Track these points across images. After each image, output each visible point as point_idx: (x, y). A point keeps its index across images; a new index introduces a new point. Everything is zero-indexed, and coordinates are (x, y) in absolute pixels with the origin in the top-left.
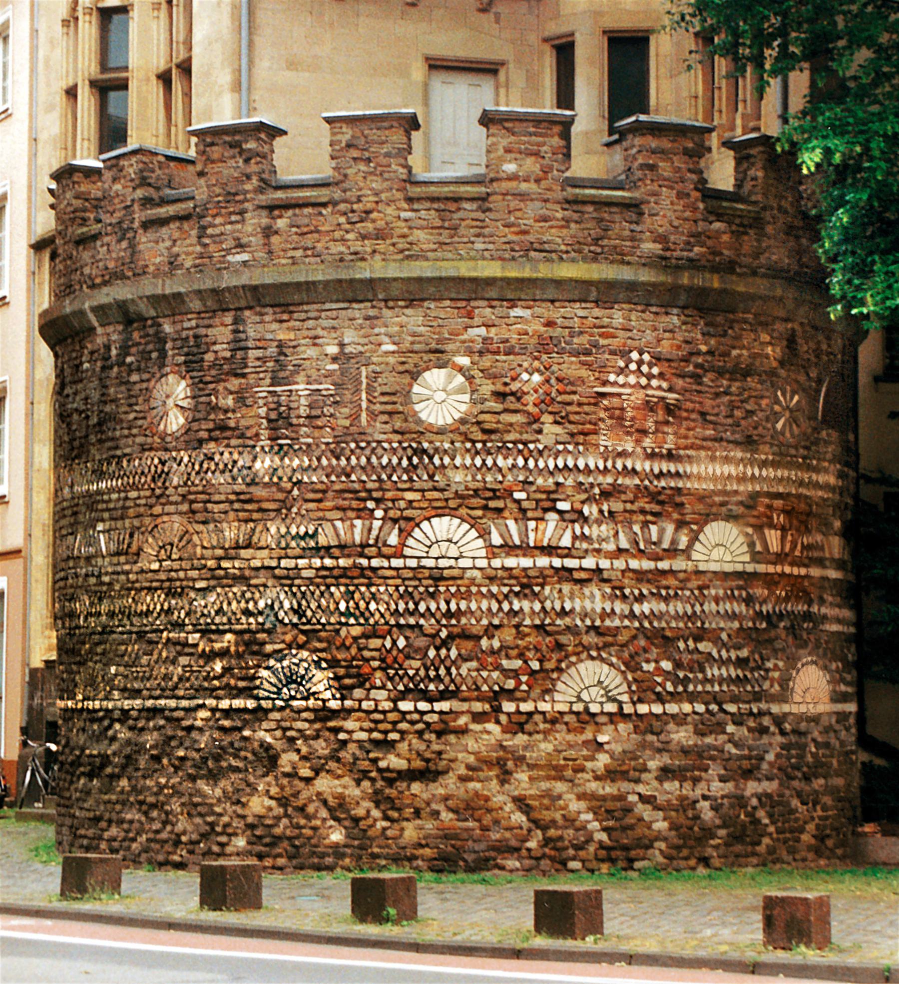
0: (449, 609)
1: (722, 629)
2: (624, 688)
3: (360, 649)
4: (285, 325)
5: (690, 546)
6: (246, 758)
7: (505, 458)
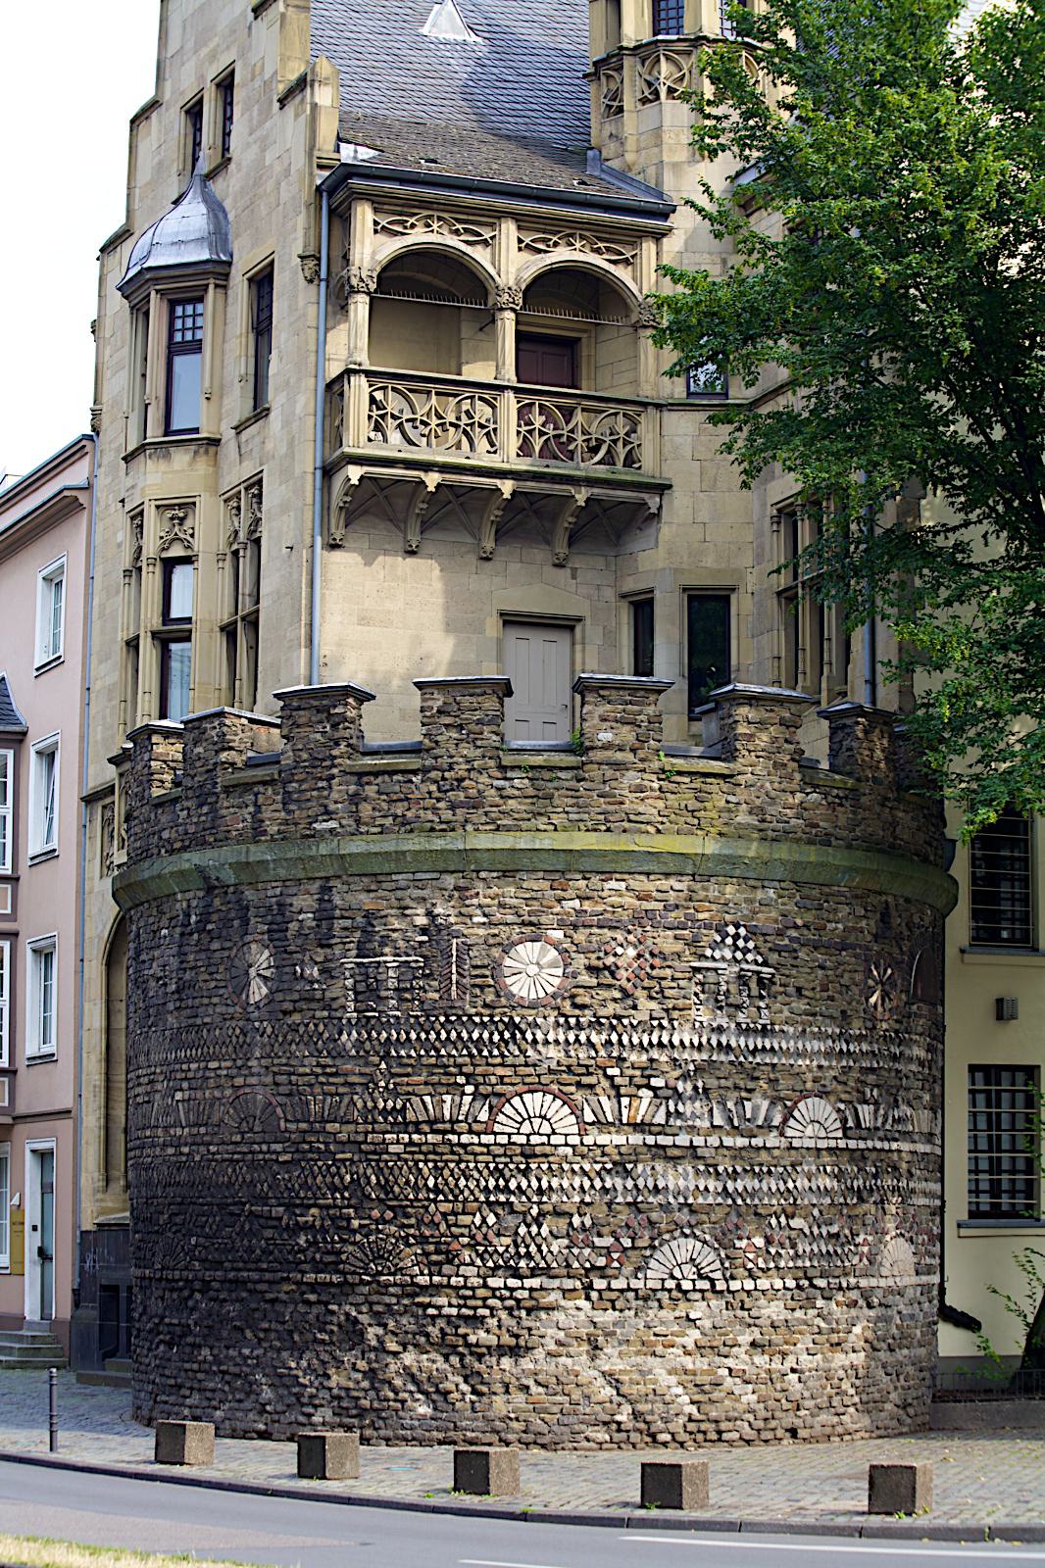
0: (540, 1186)
1: (814, 1205)
2: (717, 1264)
3: (449, 1226)
4: (372, 895)
5: (785, 1121)
6: (332, 1332)
7: (599, 1033)
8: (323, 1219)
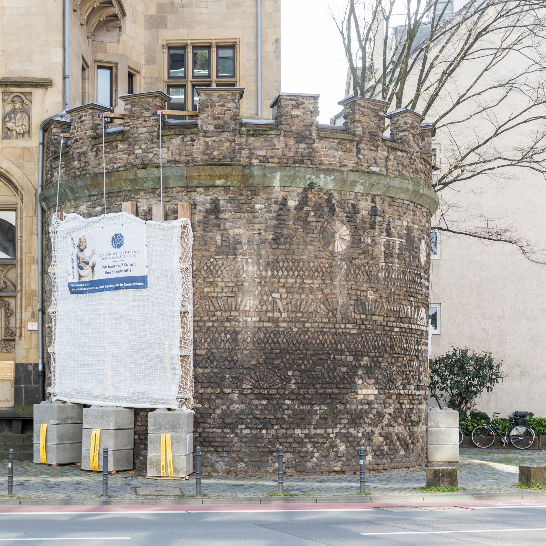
8: (371, 363)
